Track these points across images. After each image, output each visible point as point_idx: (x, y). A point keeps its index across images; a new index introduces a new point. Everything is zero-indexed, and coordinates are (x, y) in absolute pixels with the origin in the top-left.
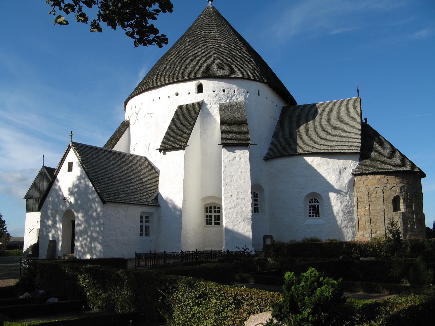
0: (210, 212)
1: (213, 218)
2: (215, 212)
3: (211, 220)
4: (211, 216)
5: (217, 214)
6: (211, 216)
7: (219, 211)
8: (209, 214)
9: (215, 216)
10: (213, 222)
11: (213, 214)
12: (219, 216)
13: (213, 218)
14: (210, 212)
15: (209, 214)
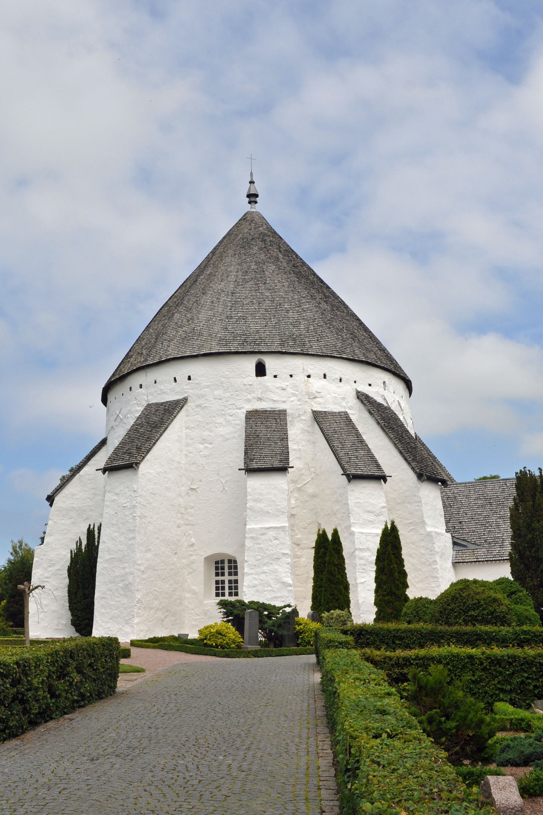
0: (223, 574)
1: (227, 585)
2: (230, 574)
3: (223, 588)
4: (223, 582)
5: (233, 578)
6: (223, 582)
7: (236, 574)
8: (220, 578)
9: (230, 582)
10: (227, 591)
11: (226, 578)
12: (236, 581)
13: (227, 585)
14: (223, 574)
15: (220, 578)
